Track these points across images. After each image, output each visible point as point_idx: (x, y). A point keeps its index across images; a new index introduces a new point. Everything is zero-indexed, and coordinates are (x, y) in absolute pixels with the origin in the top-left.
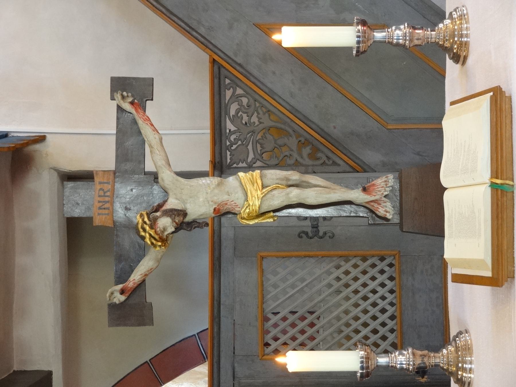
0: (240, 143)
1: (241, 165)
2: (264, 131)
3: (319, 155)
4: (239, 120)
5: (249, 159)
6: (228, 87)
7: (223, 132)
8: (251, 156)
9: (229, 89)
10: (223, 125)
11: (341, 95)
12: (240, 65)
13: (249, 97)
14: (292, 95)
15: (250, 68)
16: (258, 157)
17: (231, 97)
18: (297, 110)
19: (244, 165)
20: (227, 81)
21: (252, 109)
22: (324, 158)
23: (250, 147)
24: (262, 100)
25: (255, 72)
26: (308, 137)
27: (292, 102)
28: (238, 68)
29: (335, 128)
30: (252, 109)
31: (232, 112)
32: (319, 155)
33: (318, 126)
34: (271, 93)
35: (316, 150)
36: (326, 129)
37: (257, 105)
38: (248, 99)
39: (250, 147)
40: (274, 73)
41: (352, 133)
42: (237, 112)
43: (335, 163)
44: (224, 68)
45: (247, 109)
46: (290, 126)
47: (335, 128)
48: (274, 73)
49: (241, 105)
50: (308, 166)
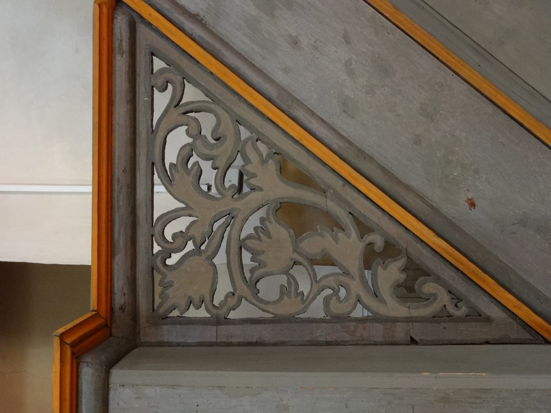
0: (190, 246)
1: (192, 313)
2: (262, 213)
3: (429, 287)
4: (190, 179)
5: (218, 298)
6: (160, 81)
7: (142, 213)
8: (224, 287)
9: (163, 89)
10: (141, 192)
11: (491, 109)
12: (195, 18)
13: (220, 111)
14: (347, 107)
15: (224, 28)
16: (243, 289)
17: (166, 111)
18: (361, 152)
19: (202, 313)
20: (158, 64)
21: (228, 145)
22: (444, 298)
23: (220, 259)
24: (256, 120)
25: (240, 40)
26: (394, 231)
27: (347, 127)
28: (189, 25)
29: (472, 205)
30: (228, 145)
31: (171, 156)
32: (429, 287)
33: (422, 198)
34: (286, 102)
35: (415, 271)
36: (446, 208)
37: (245, 133)
38: (216, 115)
39: (220, 259)
40: (295, 42)
41: (524, 222)
42: (186, 154)
43: (476, 316)
44: (149, 24)
45: (212, 147)
46: (341, 200)
47: (472, 205)
48: (295, 42)
49: (196, 133)
50: (396, 320)
